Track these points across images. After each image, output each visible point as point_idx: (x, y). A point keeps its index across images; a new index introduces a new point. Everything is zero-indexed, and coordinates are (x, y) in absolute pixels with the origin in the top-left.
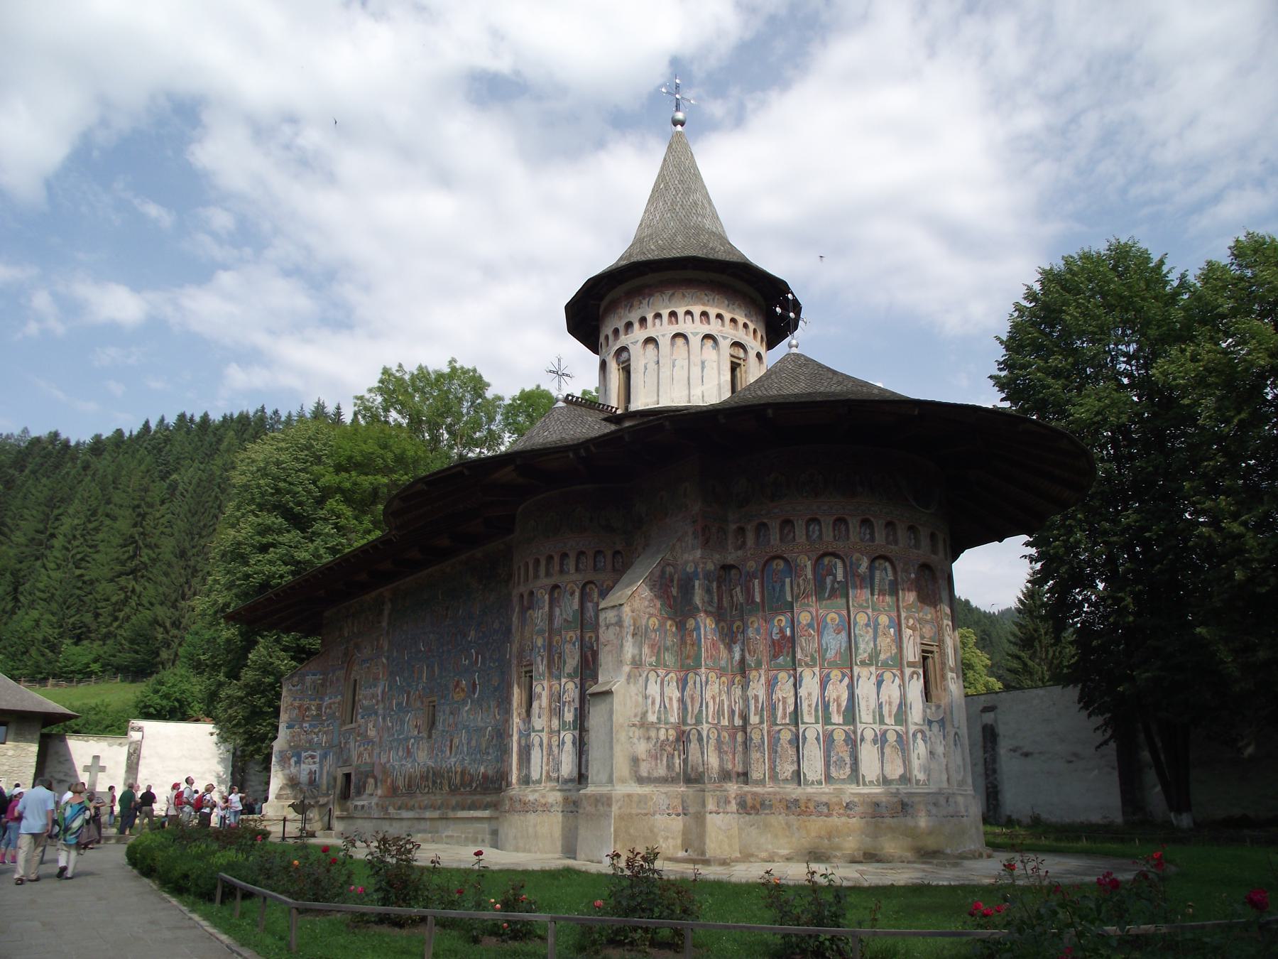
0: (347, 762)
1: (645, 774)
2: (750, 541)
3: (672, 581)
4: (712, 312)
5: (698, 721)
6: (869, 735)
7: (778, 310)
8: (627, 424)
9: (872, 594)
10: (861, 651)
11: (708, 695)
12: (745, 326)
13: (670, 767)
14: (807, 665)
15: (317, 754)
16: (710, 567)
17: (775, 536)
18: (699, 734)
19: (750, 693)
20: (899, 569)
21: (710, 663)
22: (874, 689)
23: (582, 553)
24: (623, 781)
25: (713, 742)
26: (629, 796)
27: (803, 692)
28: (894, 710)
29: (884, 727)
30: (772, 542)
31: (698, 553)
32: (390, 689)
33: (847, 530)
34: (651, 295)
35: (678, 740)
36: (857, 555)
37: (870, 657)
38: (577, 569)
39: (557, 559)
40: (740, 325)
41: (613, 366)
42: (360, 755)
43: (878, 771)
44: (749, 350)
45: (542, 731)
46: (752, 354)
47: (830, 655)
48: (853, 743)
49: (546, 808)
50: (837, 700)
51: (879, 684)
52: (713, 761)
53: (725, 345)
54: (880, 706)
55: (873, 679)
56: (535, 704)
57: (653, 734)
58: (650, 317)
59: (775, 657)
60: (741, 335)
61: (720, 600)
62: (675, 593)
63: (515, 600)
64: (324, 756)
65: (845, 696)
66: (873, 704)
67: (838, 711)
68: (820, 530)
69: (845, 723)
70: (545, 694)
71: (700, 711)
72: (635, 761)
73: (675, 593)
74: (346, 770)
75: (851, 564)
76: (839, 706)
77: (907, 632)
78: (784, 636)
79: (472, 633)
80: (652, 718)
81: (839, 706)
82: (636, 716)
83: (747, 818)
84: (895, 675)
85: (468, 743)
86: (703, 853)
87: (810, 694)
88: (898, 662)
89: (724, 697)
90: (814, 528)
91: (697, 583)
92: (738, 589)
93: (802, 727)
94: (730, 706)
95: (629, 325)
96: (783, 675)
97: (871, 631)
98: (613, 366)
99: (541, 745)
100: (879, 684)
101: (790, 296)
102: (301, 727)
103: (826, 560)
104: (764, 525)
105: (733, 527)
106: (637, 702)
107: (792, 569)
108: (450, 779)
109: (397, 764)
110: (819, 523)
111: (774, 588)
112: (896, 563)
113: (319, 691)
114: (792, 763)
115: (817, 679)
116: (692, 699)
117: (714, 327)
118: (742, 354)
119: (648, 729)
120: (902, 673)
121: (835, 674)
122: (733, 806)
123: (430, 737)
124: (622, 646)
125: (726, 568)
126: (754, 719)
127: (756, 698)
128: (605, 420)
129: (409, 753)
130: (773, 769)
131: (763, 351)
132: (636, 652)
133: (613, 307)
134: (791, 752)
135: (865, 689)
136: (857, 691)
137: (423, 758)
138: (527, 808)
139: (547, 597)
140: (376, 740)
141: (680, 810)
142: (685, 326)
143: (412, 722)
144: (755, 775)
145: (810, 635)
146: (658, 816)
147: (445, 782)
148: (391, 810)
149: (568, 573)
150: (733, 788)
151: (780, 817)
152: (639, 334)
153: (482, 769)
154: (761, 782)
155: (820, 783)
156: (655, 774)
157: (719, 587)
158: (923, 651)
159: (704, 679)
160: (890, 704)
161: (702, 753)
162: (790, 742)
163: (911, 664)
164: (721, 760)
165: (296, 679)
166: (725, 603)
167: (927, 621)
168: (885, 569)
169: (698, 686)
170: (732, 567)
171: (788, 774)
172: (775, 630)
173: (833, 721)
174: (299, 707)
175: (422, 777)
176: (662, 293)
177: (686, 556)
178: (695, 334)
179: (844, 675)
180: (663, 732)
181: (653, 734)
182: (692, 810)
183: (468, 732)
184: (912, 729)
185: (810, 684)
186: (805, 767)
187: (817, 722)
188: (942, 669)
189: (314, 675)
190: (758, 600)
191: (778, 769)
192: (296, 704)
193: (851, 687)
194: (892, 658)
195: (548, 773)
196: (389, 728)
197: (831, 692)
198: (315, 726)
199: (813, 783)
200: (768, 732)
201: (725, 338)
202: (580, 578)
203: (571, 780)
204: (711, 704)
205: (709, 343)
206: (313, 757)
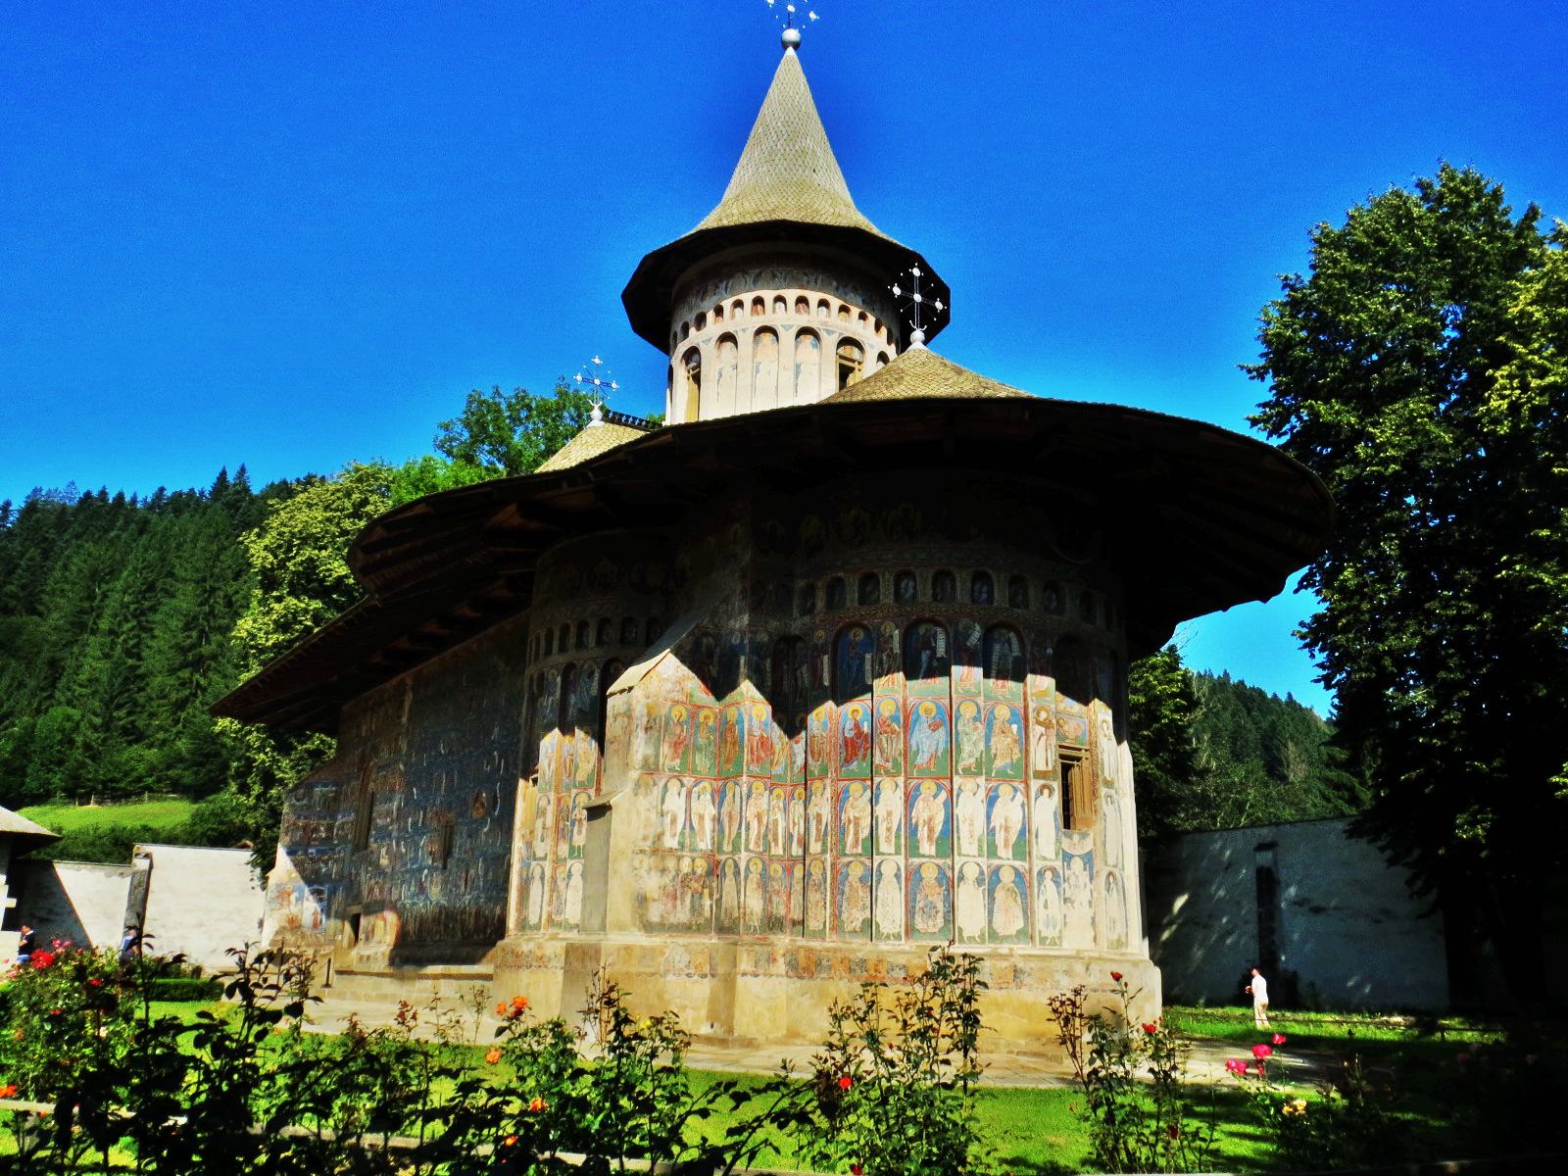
2: (820, 604)
3: (710, 656)
4: (814, 297)
5: (736, 849)
6: (971, 872)
7: (897, 291)
9: (987, 675)
10: (964, 755)
11: (750, 814)
13: (695, 910)
14: (888, 773)
15: (325, 888)
16: (763, 637)
17: (852, 596)
18: (736, 866)
19: (812, 811)
22: (983, 808)
24: (621, 928)
25: (754, 877)
26: (628, 948)
27: (880, 811)
28: (1013, 838)
29: (996, 862)
30: (848, 604)
31: (746, 618)
33: (954, 587)
34: (730, 276)
35: (710, 873)
36: (964, 622)
37: (979, 763)
38: (599, 642)
39: (573, 629)
41: (681, 373)
42: (371, 891)
43: (984, 923)
45: (545, 858)
46: (871, 355)
47: (922, 760)
48: (949, 883)
49: (542, 962)
50: (930, 821)
51: (991, 801)
52: (754, 903)
53: (830, 341)
54: (991, 832)
55: (982, 794)
57: (671, 864)
58: (727, 304)
59: (848, 761)
67: (930, 838)
68: (915, 588)
69: (938, 855)
71: (739, 834)
72: (642, 901)
75: (957, 633)
76: (931, 830)
77: (1036, 730)
78: (859, 733)
79: (496, 729)
80: (670, 842)
81: (931, 830)
82: (645, 839)
83: (798, 983)
84: (1015, 790)
85: (486, 875)
86: (730, 1031)
87: (889, 814)
88: (1022, 771)
89: (779, 816)
90: (907, 585)
92: (804, 669)
93: (877, 859)
95: (701, 320)
96: (855, 787)
98: (681, 373)
99: (542, 878)
100: (991, 801)
101: (916, 272)
102: (306, 853)
103: (922, 630)
104: (840, 580)
105: (801, 583)
106: (648, 819)
108: (463, 922)
111: (849, 667)
114: (864, 908)
115: (900, 792)
116: (730, 817)
117: (814, 317)
119: (663, 858)
120: (1027, 786)
122: (781, 966)
123: (445, 867)
124: (629, 743)
126: (815, 847)
127: (819, 817)
129: (422, 889)
130: (836, 916)
131: (891, 351)
132: (650, 751)
134: (863, 894)
135: (970, 807)
138: (518, 961)
140: (389, 870)
141: (707, 969)
142: (774, 316)
143: (427, 844)
144: (813, 924)
145: (893, 732)
146: (670, 977)
147: (458, 926)
149: (586, 647)
150: (783, 941)
151: (841, 984)
152: (714, 327)
154: (820, 934)
155: (898, 937)
156: (673, 920)
157: (775, 666)
158: (1062, 757)
159: (745, 789)
160: (1007, 829)
161: (739, 892)
162: (861, 880)
164: (768, 901)
165: (302, 791)
166: (786, 687)
168: (1009, 642)
169: (738, 799)
170: (798, 638)
171: (857, 924)
173: (921, 851)
174: (304, 828)
175: (434, 919)
176: (745, 273)
177: (732, 622)
178: (787, 328)
179: (939, 788)
181: (671, 864)
182: (721, 970)
183: (485, 861)
185: (891, 798)
186: (879, 917)
187: (898, 853)
188: (1094, 783)
189: (326, 785)
190: (826, 683)
191: (845, 916)
193: (950, 805)
194: (1013, 766)
195: (550, 916)
196: (402, 856)
197: (921, 812)
199: (888, 937)
200: (833, 865)
201: (829, 332)
204: (754, 824)
205: (808, 339)
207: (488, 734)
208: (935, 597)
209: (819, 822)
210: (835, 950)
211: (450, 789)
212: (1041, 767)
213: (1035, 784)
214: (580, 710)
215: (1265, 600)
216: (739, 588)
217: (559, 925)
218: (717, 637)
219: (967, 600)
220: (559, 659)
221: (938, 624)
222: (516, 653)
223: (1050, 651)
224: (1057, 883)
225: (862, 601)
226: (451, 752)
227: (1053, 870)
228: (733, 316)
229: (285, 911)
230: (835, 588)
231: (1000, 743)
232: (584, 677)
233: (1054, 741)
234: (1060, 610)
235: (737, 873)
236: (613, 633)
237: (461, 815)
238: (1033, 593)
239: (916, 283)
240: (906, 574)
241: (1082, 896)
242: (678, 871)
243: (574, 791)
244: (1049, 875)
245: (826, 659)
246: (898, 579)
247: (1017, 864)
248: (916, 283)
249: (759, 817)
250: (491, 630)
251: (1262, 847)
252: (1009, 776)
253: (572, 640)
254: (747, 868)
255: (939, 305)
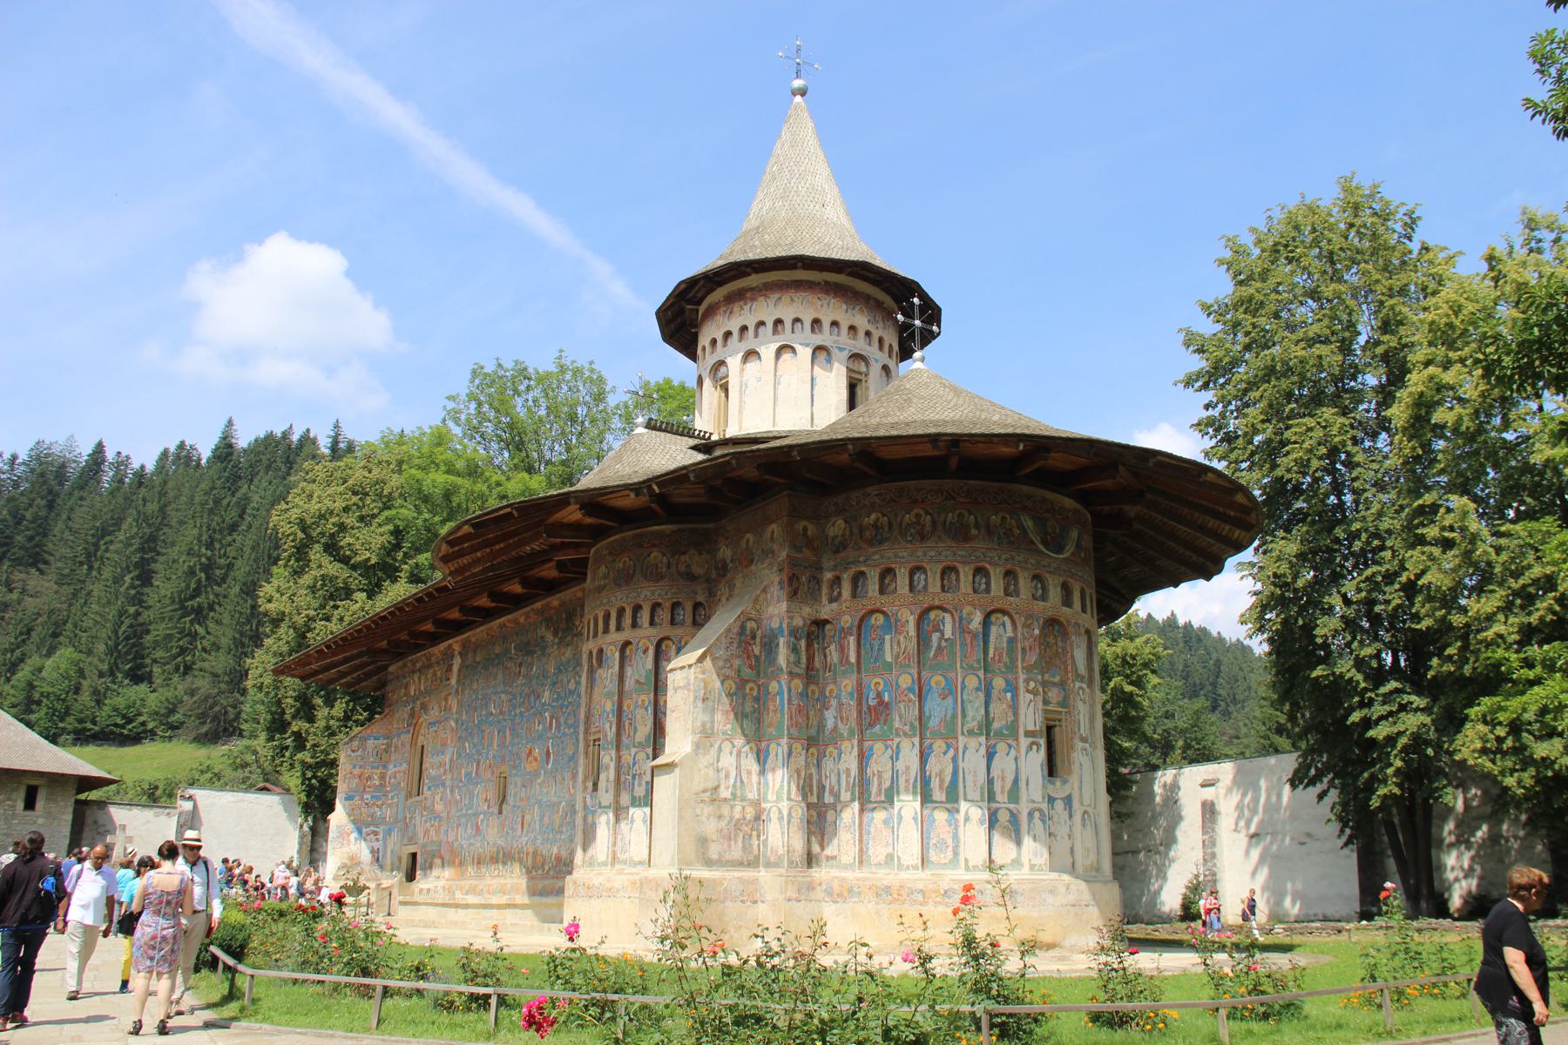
0: (412, 840)
1: (715, 856)
3: (754, 637)
5: (779, 799)
7: (900, 317)
8: (718, 452)
12: (868, 334)
13: (746, 848)
14: (905, 734)
15: (381, 829)
16: (798, 622)
17: (873, 587)
18: (780, 812)
20: (1019, 626)
21: (794, 732)
22: (984, 762)
23: (659, 605)
25: (796, 821)
28: (1008, 785)
29: (994, 805)
31: (784, 606)
32: (459, 755)
33: (958, 580)
34: (753, 299)
35: (758, 818)
36: (968, 608)
38: (652, 623)
39: (629, 612)
40: (861, 334)
42: (426, 832)
44: (872, 362)
46: (875, 369)
47: (933, 723)
50: (940, 774)
51: (990, 756)
54: (990, 782)
55: (983, 751)
56: (603, 777)
57: (726, 811)
59: (871, 725)
60: (860, 345)
61: (810, 659)
62: (757, 652)
63: (585, 657)
64: (388, 833)
65: (950, 769)
66: (982, 777)
70: (612, 765)
72: (703, 841)
73: (757, 652)
74: (412, 849)
76: (942, 781)
77: (1025, 698)
78: (881, 702)
79: (547, 694)
81: (942, 781)
82: (704, 791)
85: (542, 817)
87: (908, 768)
89: (813, 770)
91: (782, 641)
94: (820, 781)
95: (728, 334)
96: (878, 746)
97: (982, 695)
100: (990, 756)
101: (916, 300)
103: (932, 615)
104: (863, 573)
105: (828, 575)
107: (893, 625)
109: (465, 843)
110: (925, 572)
112: (1016, 617)
113: (383, 757)
114: (887, 844)
115: (916, 750)
118: (863, 369)
121: (939, 745)
123: (500, 812)
125: (820, 624)
126: (845, 796)
127: (848, 770)
128: (694, 448)
133: (711, 311)
134: (885, 833)
136: (961, 765)
137: (493, 836)
139: (617, 654)
140: (444, 815)
143: (484, 792)
144: (845, 859)
148: (458, 895)
153: (555, 851)
156: (728, 856)
157: (809, 646)
160: (1003, 779)
162: (885, 822)
163: (1028, 734)
165: (355, 743)
166: (817, 664)
167: (1054, 684)
170: (826, 622)
171: (882, 858)
172: (872, 695)
177: (771, 609)
179: (949, 746)
180: (738, 809)
181: (726, 811)
182: (769, 897)
183: (540, 806)
184: (1024, 808)
190: (853, 659)
191: (871, 852)
192: (357, 771)
194: (1007, 728)
195: (614, 852)
197: (933, 765)
198: (378, 798)
201: (841, 349)
202: (654, 633)
203: (641, 863)
205: (822, 356)
206: (376, 833)
207: (538, 697)
208: (943, 587)
209: (848, 775)
210: (865, 879)
211: (502, 745)
212: (1031, 727)
213: (1024, 742)
214: (637, 682)
215: (1208, 578)
216: (776, 579)
217: (625, 862)
218: (758, 621)
219: (970, 590)
220: (616, 637)
221: (944, 610)
222: (567, 625)
223: (1037, 632)
224: (1043, 821)
225: (882, 592)
226: (501, 713)
227: (1040, 810)
228: (756, 335)
229: (345, 849)
230: (859, 578)
231: (998, 709)
232: (640, 652)
233: (1040, 706)
234: (1044, 598)
235: (781, 818)
236: (664, 615)
237: (514, 767)
238: (1024, 584)
239: (916, 311)
240: (919, 568)
241: (1062, 831)
242: (732, 817)
243: (633, 750)
244: (1037, 814)
245: (852, 640)
246: (912, 573)
247: (1012, 806)
248: (916, 311)
249: (798, 771)
250: (538, 605)
251: (1206, 784)
252: (1002, 735)
253: (628, 620)
254: (790, 814)
255: (935, 328)
